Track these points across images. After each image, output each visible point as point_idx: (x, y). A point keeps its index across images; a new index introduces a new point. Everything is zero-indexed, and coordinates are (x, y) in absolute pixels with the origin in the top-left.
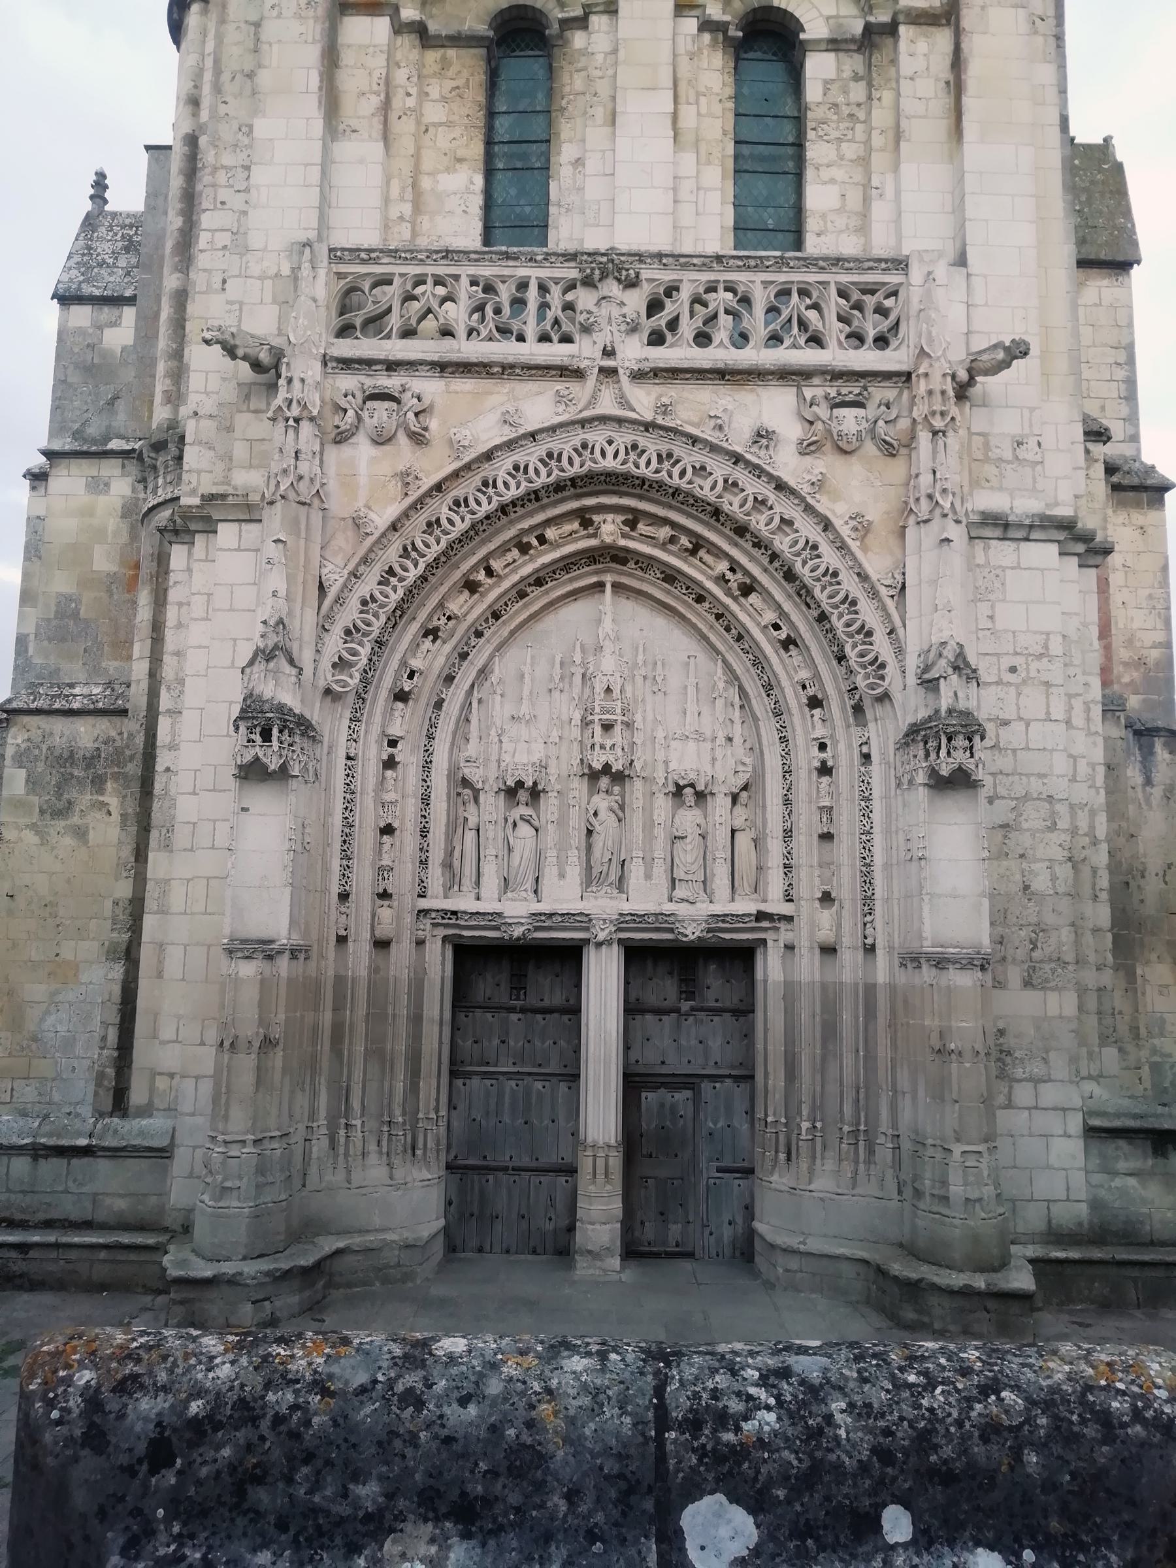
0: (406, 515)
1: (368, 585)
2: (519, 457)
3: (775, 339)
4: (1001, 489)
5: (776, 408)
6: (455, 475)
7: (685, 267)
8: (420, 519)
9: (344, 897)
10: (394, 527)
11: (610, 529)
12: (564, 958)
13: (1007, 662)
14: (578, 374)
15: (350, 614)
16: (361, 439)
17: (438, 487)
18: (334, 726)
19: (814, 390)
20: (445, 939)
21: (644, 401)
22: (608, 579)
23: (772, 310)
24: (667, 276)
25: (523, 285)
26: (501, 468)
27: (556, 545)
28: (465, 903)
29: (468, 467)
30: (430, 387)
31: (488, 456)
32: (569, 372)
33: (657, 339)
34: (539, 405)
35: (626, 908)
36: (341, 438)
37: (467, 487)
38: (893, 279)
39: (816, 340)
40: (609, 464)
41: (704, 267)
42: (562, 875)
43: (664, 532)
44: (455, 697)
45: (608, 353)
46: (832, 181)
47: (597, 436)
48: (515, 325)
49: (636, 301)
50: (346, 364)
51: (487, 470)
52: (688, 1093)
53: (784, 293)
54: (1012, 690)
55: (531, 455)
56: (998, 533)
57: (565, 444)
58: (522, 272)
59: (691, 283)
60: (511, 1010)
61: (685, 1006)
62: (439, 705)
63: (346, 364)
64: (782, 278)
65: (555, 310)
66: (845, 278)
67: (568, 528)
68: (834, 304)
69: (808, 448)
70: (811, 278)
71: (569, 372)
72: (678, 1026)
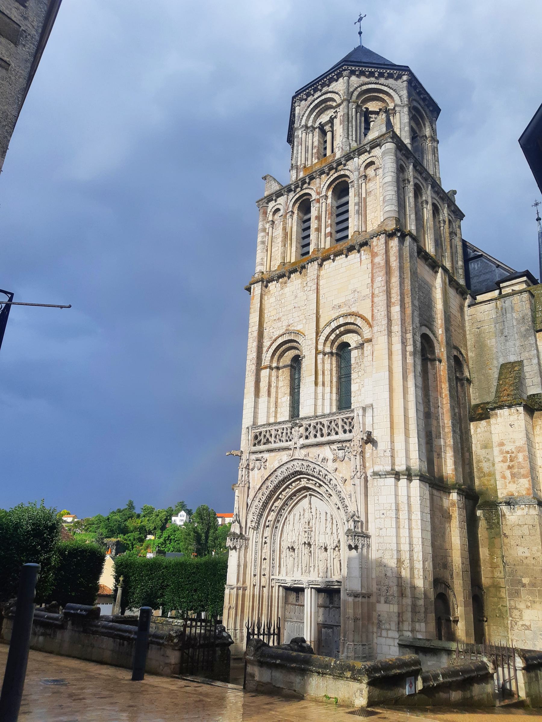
0: (261, 486)
1: (256, 503)
2: (282, 470)
3: (329, 434)
4: (381, 465)
5: (326, 452)
6: (270, 476)
7: (311, 420)
8: (264, 487)
9: (255, 575)
10: (260, 489)
11: (303, 483)
12: (302, 590)
13: (382, 512)
14: (291, 449)
15: (253, 510)
16: (256, 469)
17: (267, 479)
18: (251, 535)
19: (334, 446)
20: (279, 586)
21: (300, 454)
22: (307, 493)
23: (329, 427)
24: (308, 423)
25: (283, 429)
26: (278, 472)
27: (295, 487)
28: (280, 577)
29: (272, 473)
30: (266, 455)
31: (275, 471)
32: (288, 449)
33: (307, 438)
34: (284, 457)
35: (309, 579)
36: (252, 469)
37: (273, 478)
38: (352, 415)
39: (337, 433)
40: (298, 469)
41: (315, 419)
42: (298, 570)
43: (314, 482)
44: (280, 526)
45: (295, 443)
46: (357, 382)
47: (295, 463)
48: (282, 439)
49: (302, 430)
50: (254, 453)
51: (276, 473)
52: (331, 630)
53: (331, 423)
54: (383, 520)
55: (284, 469)
56: (379, 477)
57: (289, 465)
58: (283, 427)
59: (313, 423)
60: (296, 605)
61: (331, 606)
62: (276, 528)
63: (254, 453)
64: (330, 419)
65: (289, 434)
66: (342, 417)
67: (297, 483)
68: (340, 423)
69: (334, 460)
70: (335, 418)
71: (288, 449)
72: (329, 611)
